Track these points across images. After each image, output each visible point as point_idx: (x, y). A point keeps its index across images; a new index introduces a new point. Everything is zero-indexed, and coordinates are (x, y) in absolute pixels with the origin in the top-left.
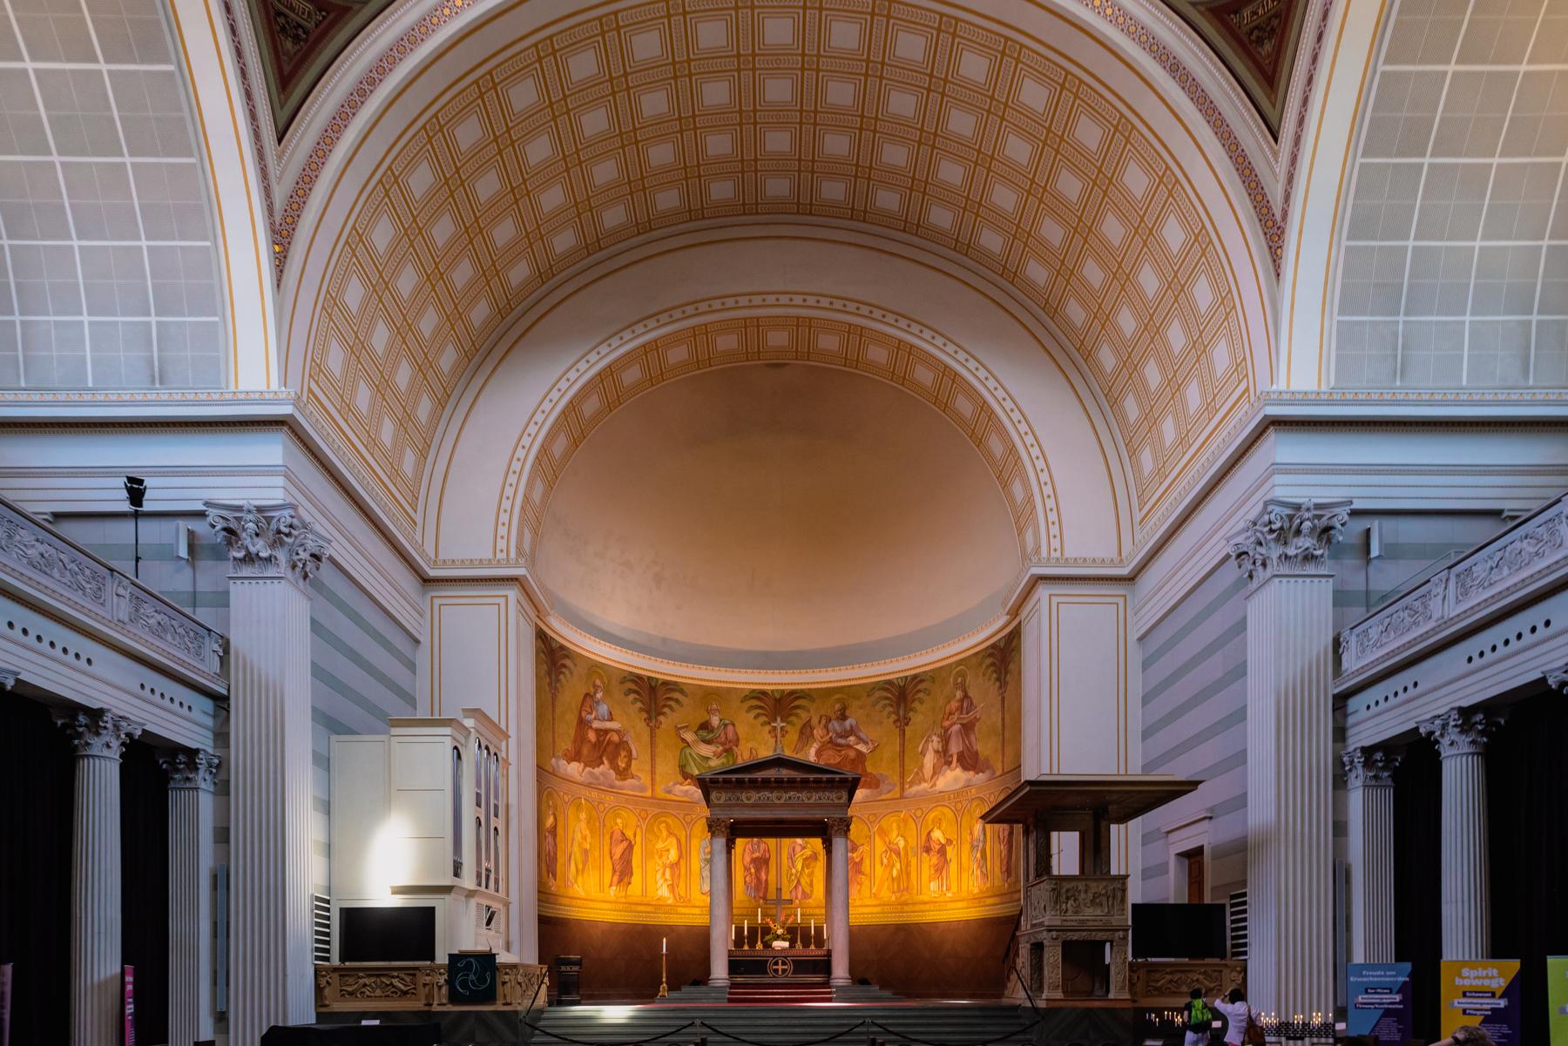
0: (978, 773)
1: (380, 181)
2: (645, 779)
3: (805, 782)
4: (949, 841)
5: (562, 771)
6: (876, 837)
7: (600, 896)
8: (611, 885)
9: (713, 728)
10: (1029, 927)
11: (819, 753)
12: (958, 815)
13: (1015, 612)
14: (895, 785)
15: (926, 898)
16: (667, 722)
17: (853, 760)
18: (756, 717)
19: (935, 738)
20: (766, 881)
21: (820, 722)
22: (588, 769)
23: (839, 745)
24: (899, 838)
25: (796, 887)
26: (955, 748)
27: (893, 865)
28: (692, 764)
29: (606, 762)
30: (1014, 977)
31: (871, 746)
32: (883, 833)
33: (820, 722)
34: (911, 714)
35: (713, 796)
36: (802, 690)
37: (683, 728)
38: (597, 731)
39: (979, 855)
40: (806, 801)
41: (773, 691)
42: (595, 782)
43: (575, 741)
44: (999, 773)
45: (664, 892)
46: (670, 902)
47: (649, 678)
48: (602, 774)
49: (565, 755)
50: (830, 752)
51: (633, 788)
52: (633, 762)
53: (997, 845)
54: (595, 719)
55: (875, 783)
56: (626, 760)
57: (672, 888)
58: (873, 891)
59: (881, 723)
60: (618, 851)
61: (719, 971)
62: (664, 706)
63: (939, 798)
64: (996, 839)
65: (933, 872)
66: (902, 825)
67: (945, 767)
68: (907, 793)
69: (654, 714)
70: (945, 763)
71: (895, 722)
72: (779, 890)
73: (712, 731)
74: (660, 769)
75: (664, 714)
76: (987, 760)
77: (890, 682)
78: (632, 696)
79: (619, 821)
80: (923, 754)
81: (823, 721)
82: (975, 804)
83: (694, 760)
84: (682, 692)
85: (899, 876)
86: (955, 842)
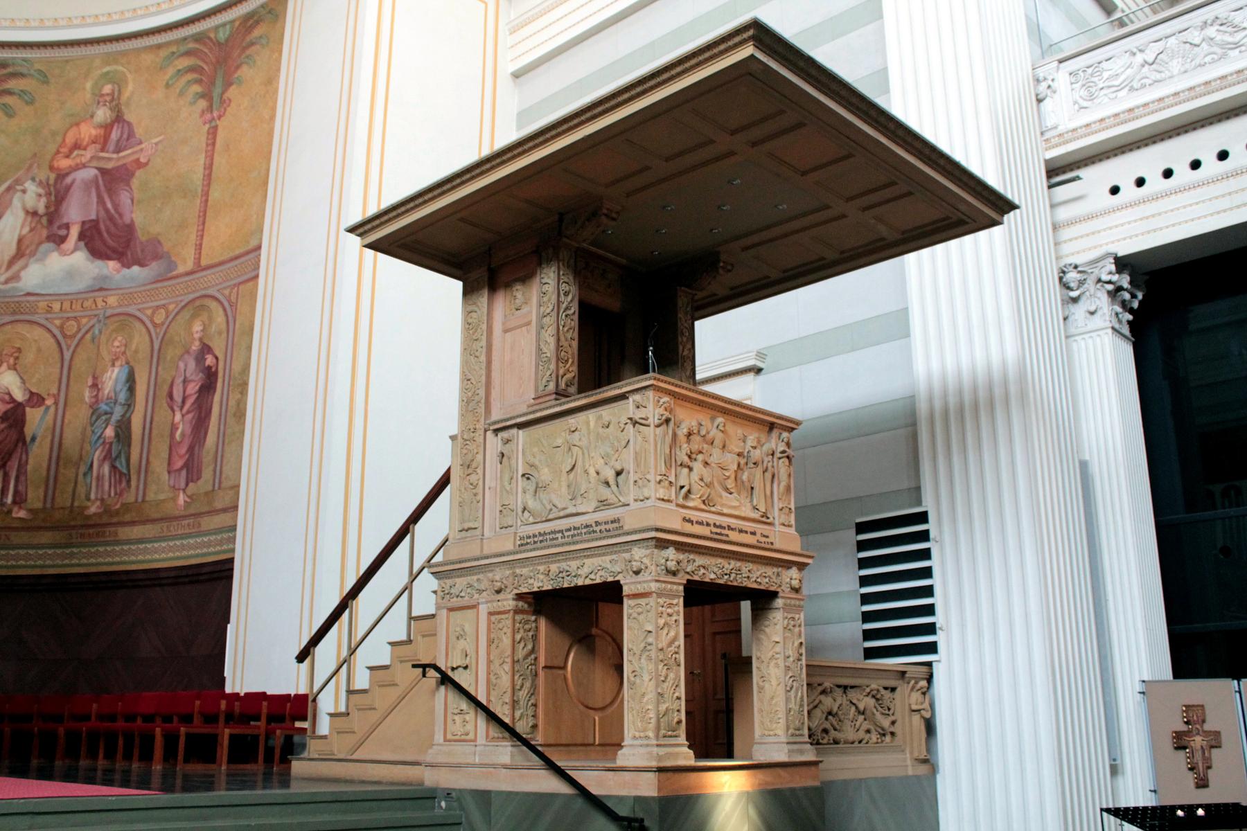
0: (129, 267)
19: (31, 188)
26: (76, 212)
39: (110, 432)
64: (163, 403)
67: (51, 245)
76: (156, 242)
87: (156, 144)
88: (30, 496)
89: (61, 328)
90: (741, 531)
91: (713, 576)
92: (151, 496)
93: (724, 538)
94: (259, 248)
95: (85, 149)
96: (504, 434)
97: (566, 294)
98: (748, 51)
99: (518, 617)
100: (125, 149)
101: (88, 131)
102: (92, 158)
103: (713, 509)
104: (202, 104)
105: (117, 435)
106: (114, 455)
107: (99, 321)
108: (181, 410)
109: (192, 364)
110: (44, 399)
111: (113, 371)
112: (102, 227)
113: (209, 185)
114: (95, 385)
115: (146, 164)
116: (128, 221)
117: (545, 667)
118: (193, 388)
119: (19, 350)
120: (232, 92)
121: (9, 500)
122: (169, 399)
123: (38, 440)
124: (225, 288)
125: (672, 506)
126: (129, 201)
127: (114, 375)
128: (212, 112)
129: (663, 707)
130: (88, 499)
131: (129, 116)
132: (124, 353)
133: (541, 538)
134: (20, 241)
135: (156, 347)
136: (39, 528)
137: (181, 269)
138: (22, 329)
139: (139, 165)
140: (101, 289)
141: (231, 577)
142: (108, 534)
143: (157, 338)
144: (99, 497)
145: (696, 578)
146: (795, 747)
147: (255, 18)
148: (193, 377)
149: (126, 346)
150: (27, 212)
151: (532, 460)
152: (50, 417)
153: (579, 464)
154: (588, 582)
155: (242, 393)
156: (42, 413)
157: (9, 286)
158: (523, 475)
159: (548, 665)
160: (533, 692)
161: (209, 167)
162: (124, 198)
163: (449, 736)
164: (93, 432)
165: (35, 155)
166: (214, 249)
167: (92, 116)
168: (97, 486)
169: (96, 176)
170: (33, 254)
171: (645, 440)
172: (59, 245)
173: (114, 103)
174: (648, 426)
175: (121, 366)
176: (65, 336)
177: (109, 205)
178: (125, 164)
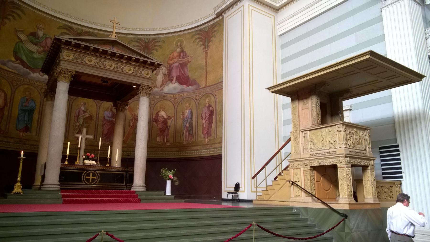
0: (188, 86)
3: (129, 59)
9: (39, 37)
13: (220, 14)
26: (175, 74)
39: (187, 125)
62: (10, 15)
70: (169, 80)
84: (22, 11)
87: (192, 57)
88: (170, 140)
89: (174, 101)
90: (361, 153)
91: (356, 163)
92: (199, 139)
93: (357, 155)
94: (222, 82)
95: (175, 59)
96: (305, 132)
98: (368, 56)
99: (311, 171)
100: (184, 59)
101: (175, 54)
102: (177, 60)
103: (355, 148)
104: (203, 47)
105: (189, 126)
106: (189, 131)
107: (183, 99)
108: (205, 119)
109: (207, 109)
110: (171, 118)
111: (187, 111)
112: (181, 77)
113: (207, 66)
115: (191, 61)
116: (187, 76)
117: (316, 182)
118: (207, 115)
119: (165, 106)
120: (210, 44)
121: (165, 141)
122: (201, 117)
123: (171, 127)
124: (213, 91)
125: (347, 149)
126: (187, 71)
127: (187, 112)
128: (206, 49)
129: (349, 191)
130: (184, 141)
131: (185, 50)
132: (189, 107)
133: (316, 155)
134: (162, 81)
135: (197, 105)
137: (202, 87)
138: (165, 101)
139: (189, 62)
140: (182, 92)
141: (222, 158)
142: (189, 148)
143: (197, 103)
144: (186, 140)
145: (353, 164)
146: (375, 200)
147: (215, 25)
148: (207, 112)
149: (190, 105)
150: (163, 74)
151: (312, 138)
152: (173, 122)
153: (324, 139)
154: (328, 164)
155: (220, 116)
156: (171, 121)
157: (161, 92)
158: (310, 141)
159: (317, 181)
160: (314, 187)
161: (206, 62)
162: (186, 70)
163: (295, 196)
164: (183, 125)
165: (164, 60)
166: (209, 83)
167: (176, 50)
168: (186, 137)
169: (178, 65)
170: (166, 84)
171: (341, 135)
172: (171, 82)
173: (181, 47)
174: (341, 132)
175: (189, 110)
176: (175, 103)
177: (182, 72)
178: (185, 62)
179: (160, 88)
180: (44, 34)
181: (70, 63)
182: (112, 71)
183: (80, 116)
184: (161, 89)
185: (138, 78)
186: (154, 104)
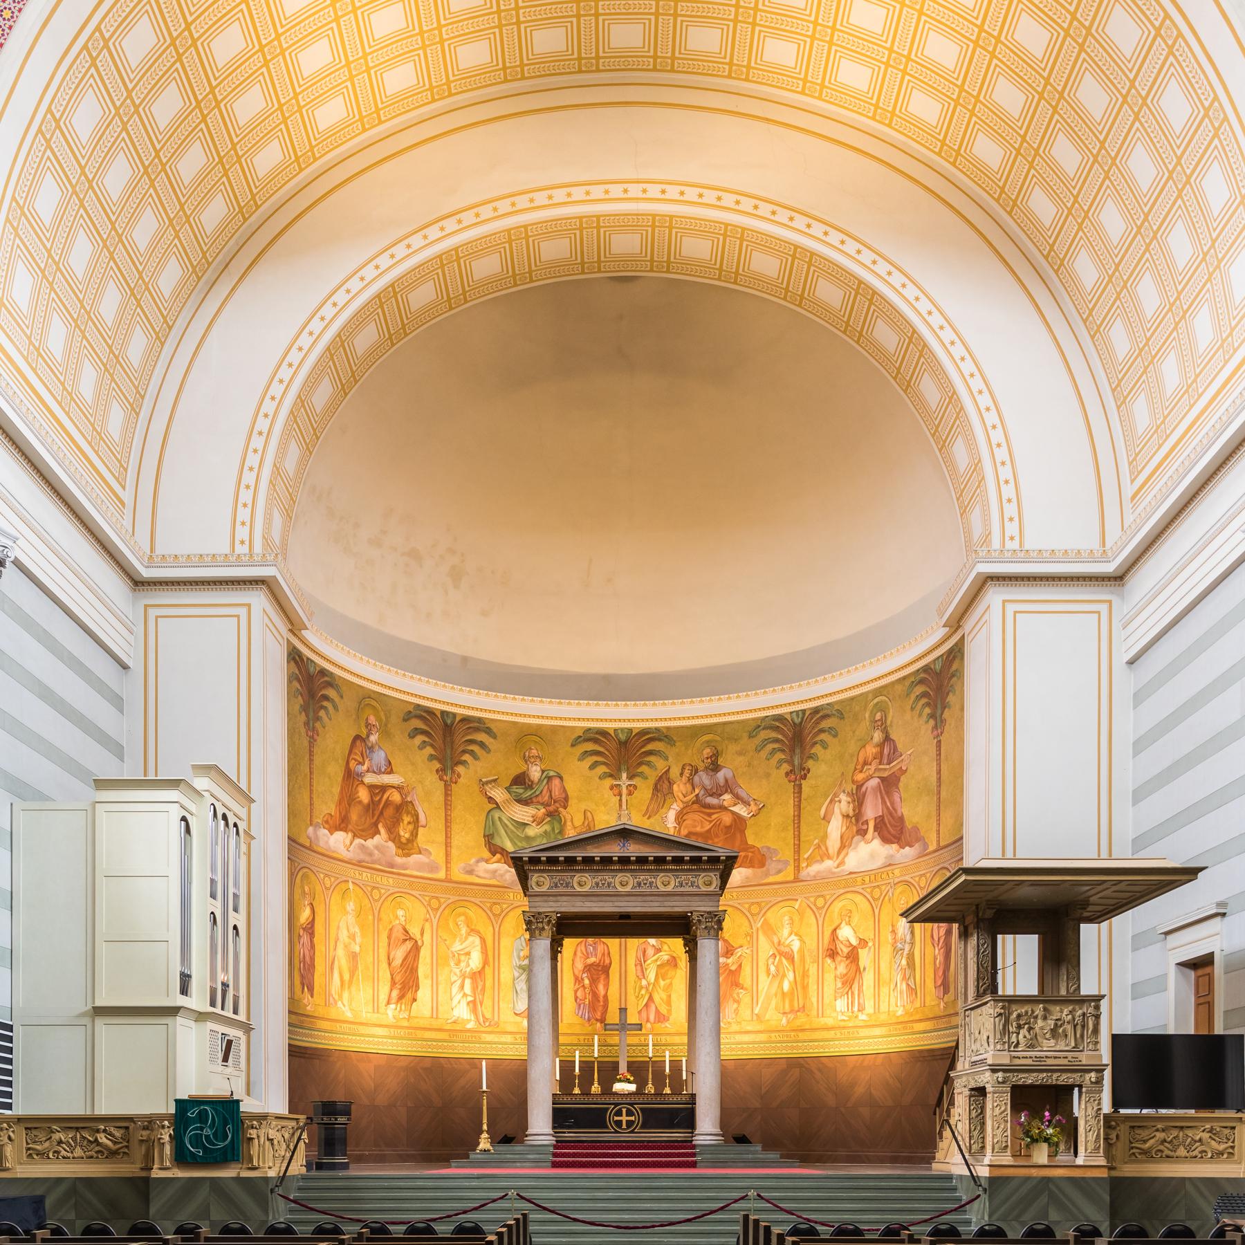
1: (85, 47)
2: (438, 855)
3: (660, 861)
4: (863, 943)
5: (322, 843)
6: (760, 933)
7: (374, 1018)
8: (388, 1003)
10: (967, 1066)
11: (680, 818)
12: (875, 904)
13: (956, 623)
14: (786, 863)
15: (830, 1022)
16: (468, 774)
17: (728, 828)
18: (592, 767)
19: (843, 797)
20: (606, 996)
21: (682, 774)
22: (358, 841)
23: (709, 806)
24: (793, 937)
25: (647, 1005)
27: (784, 976)
28: (503, 832)
29: (382, 830)
30: (947, 1133)
31: (753, 808)
32: (769, 930)
33: (682, 774)
34: (810, 764)
35: (534, 879)
36: (657, 729)
37: (487, 783)
38: (371, 788)
39: (904, 962)
40: (662, 888)
41: (615, 730)
42: (367, 858)
43: (340, 802)
44: (931, 848)
45: (462, 1012)
46: (470, 1026)
47: (443, 712)
48: (377, 847)
49: (327, 822)
50: (697, 816)
51: (420, 867)
52: (421, 830)
53: (929, 948)
54: (368, 771)
55: (759, 860)
56: (411, 827)
57: (473, 1006)
58: (756, 1011)
59: (768, 775)
60: (399, 954)
61: (540, 1124)
62: (464, 752)
63: (851, 881)
65: (839, 985)
66: (796, 918)
67: (858, 838)
68: (803, 874)
69: (449, 764)
71: (787, 774)
72: (623, 1011)
73: (531, 787)
74: (456, 841)
75: (464, 763)
77: (780, 718)
78: (419, 739)
79: (400, 913)
80: (827, 818)
81: (687, 773)
82: (899, 889)
83: (505, 826)
84: (489, 731)
85: (792, 993)
86: (870, 944)
89: (871, 893)
90: (1055, 1058)
97: (983, 945)
98: (963, 878)
114: (893, 931)
119: (850, 911)
134: (841, 837)
136: (873, 1026)
140: (890, 865)
150: (843, 816)
179: (838, 857)
180: (543, 772)
181: (546, 898)
182: (629, 895)
183: (649, 962)
184: (837, 862)
185: (686, 898)
186: (823, 907)
